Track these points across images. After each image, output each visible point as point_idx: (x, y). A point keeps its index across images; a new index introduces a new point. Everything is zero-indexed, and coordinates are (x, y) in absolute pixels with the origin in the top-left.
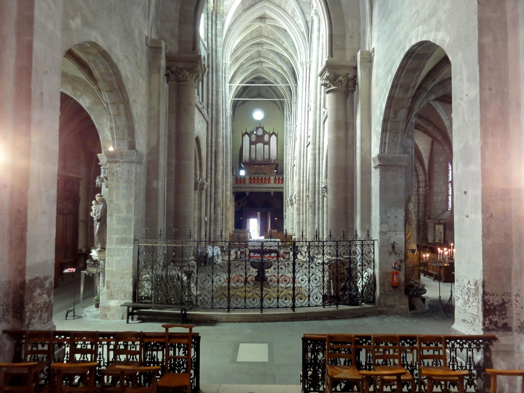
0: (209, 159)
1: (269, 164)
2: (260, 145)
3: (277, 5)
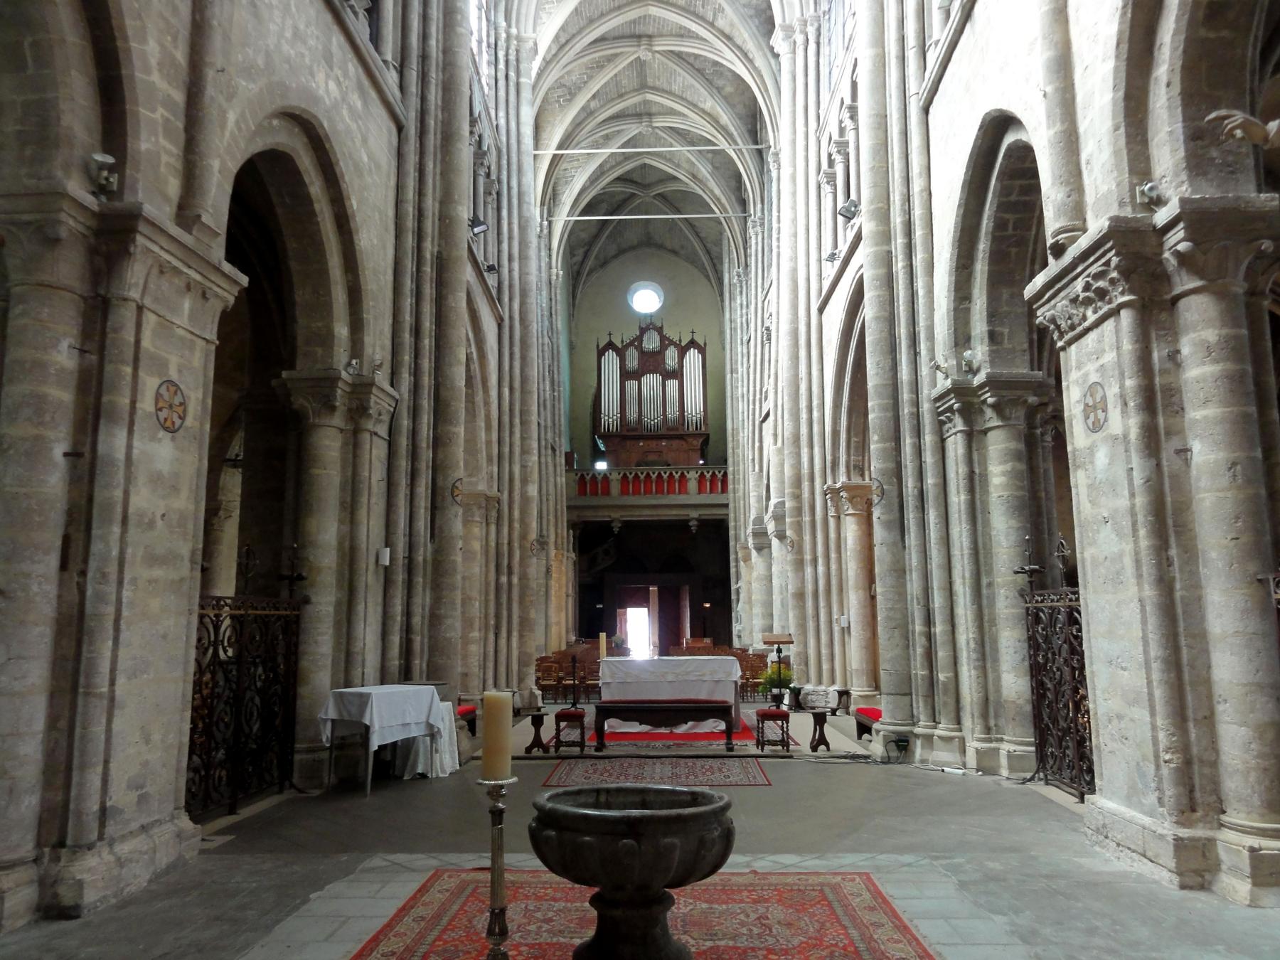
0: (408, 284)
1: (681, 437)
2: (651, 382)
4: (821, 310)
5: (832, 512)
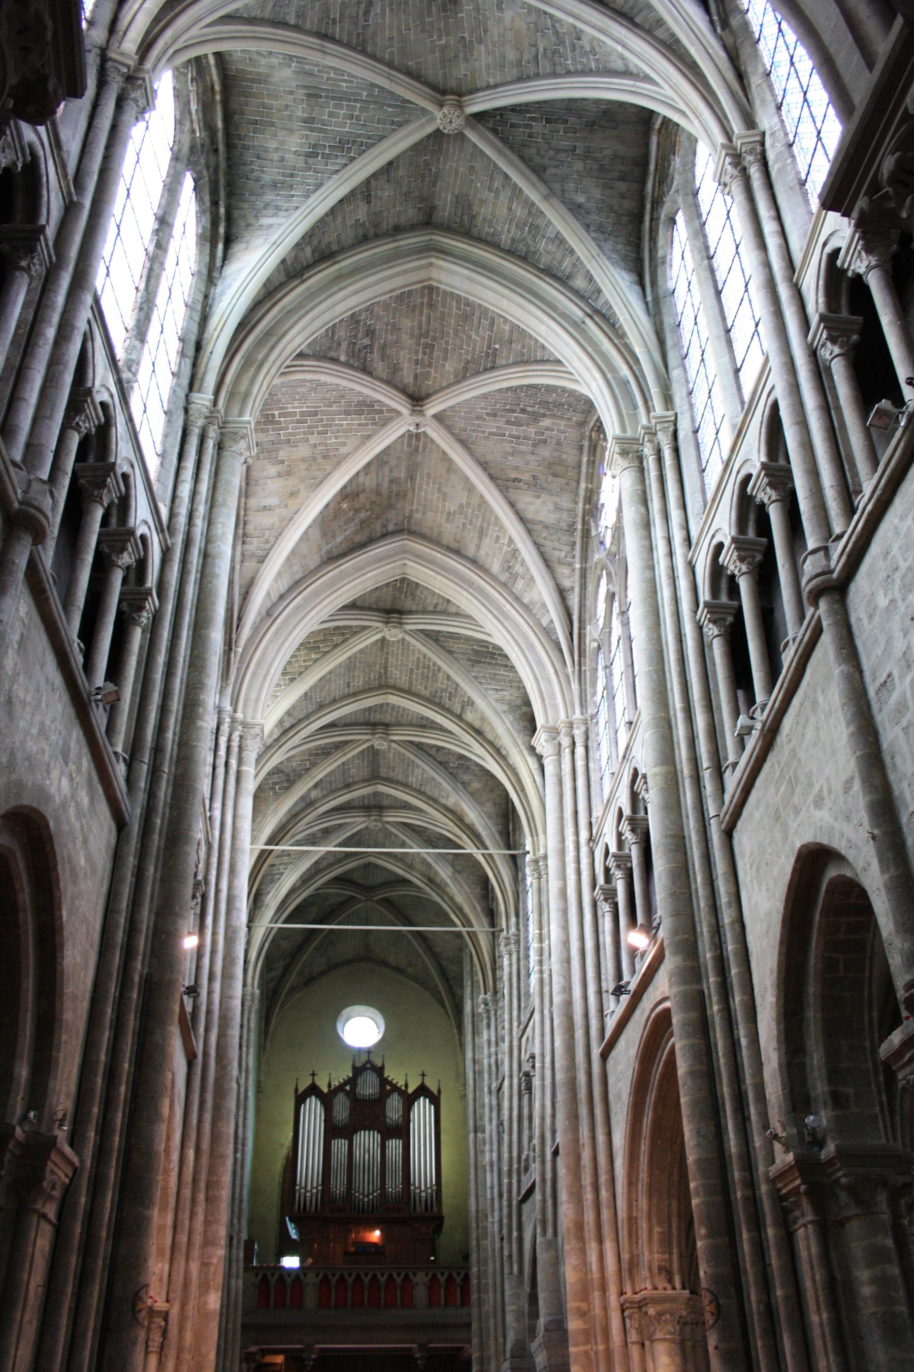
2: (367, 1141)
3: (449, 549)
4: (604, 1056)
5: (633, 1336)
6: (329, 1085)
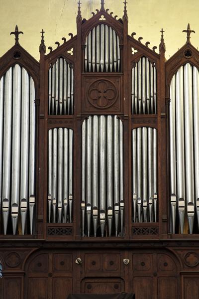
1: (162, 247)
2: (101, 130)
6: (42, 48)
